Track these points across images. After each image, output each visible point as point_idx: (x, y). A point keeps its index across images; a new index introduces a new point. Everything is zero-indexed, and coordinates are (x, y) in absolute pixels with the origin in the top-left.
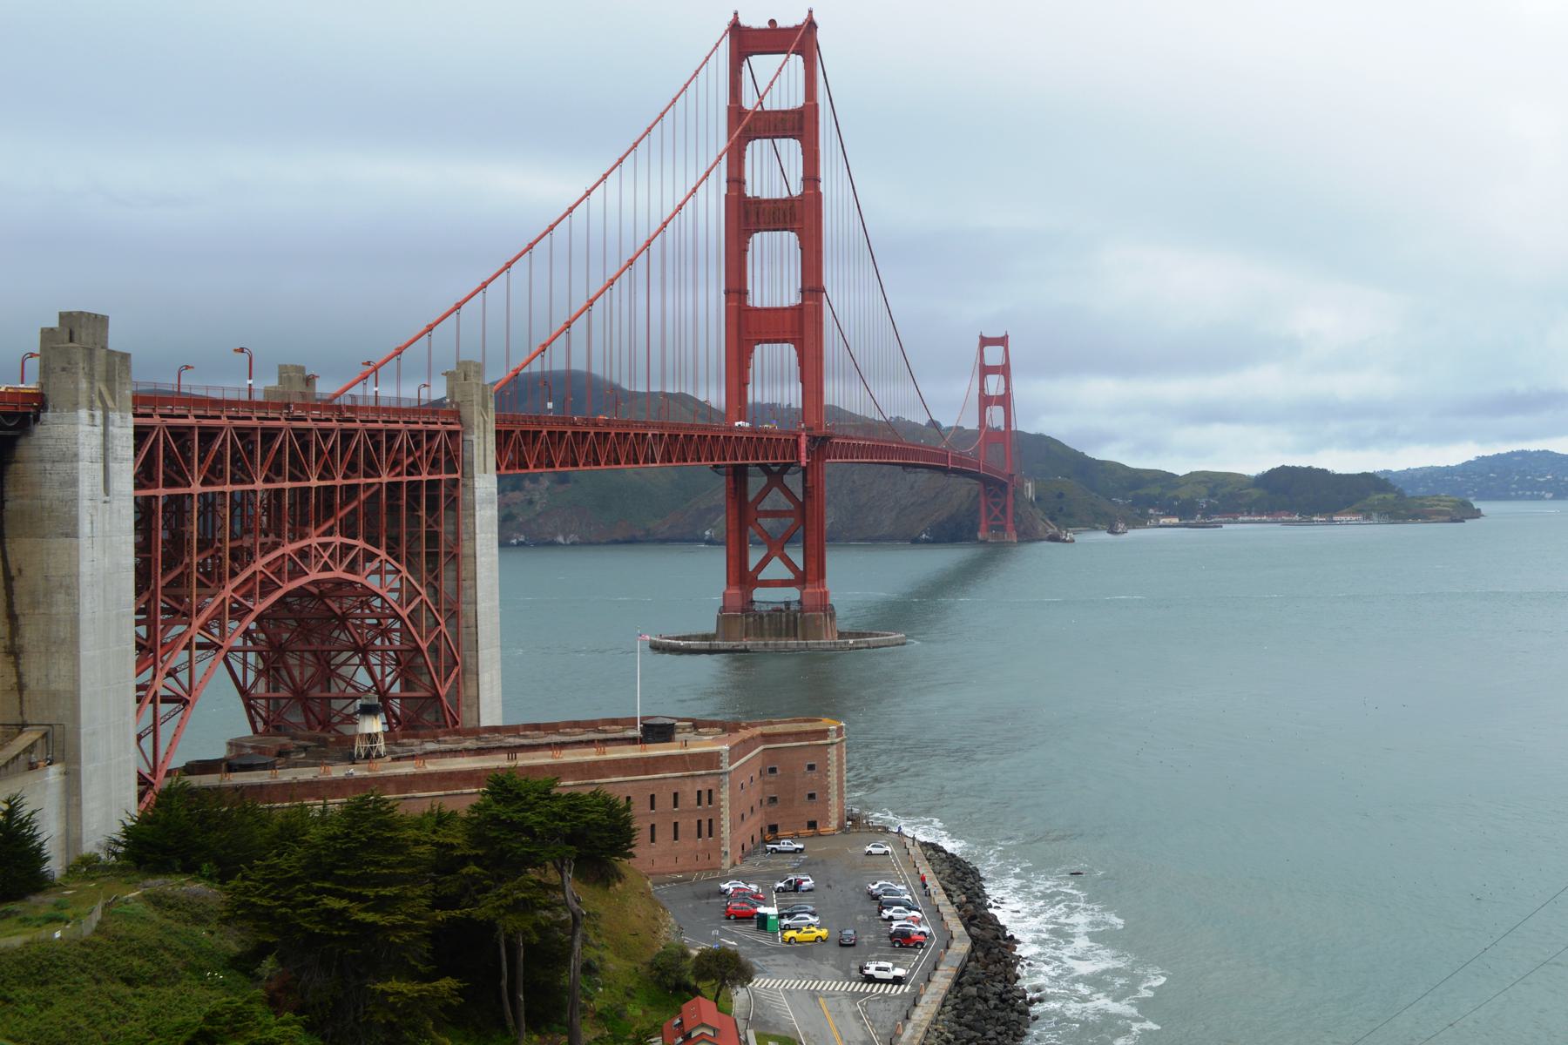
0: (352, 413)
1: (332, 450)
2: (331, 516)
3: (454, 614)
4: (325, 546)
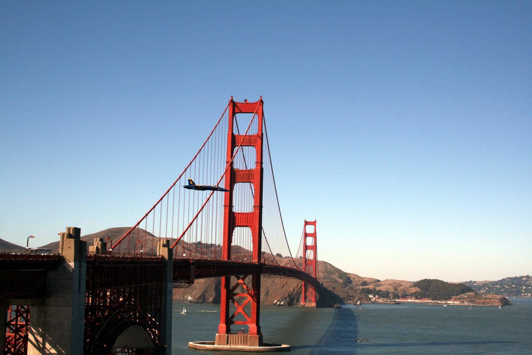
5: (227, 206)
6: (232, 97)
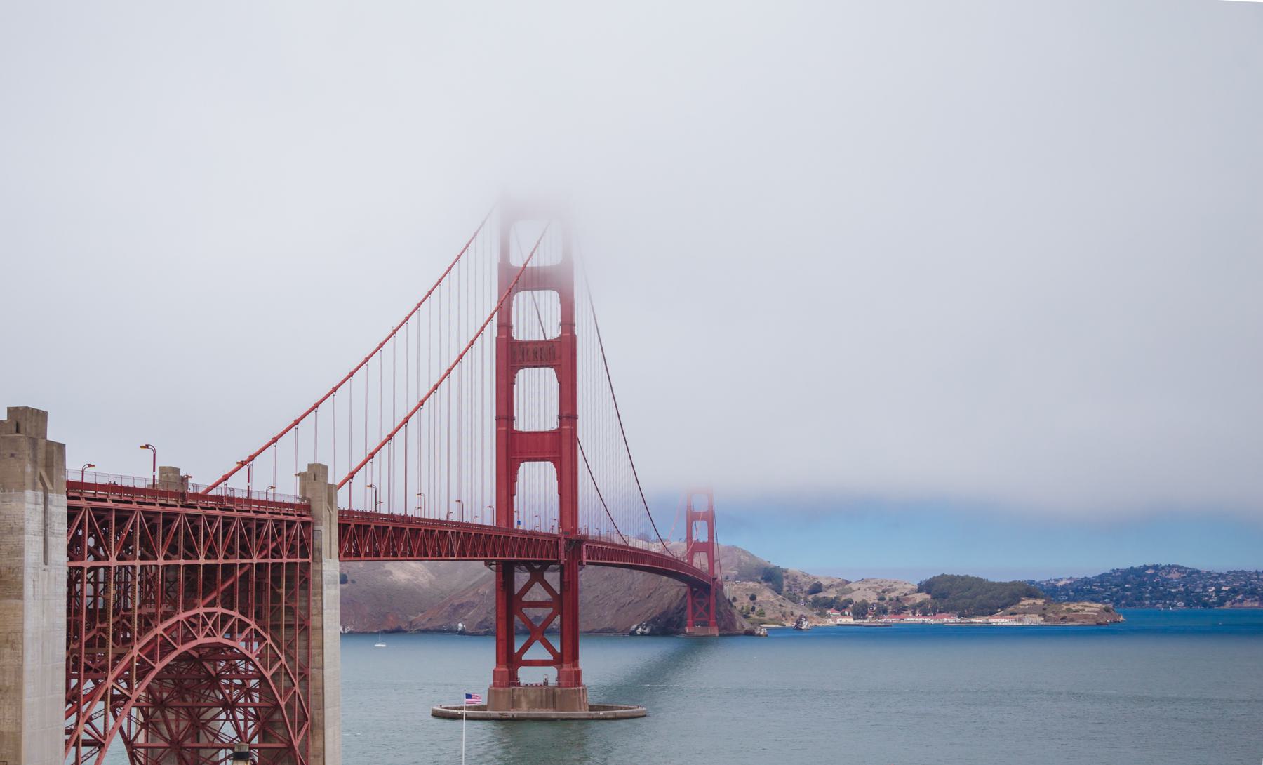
0: (231, 503)
2: (215, 590)
3: (304, 677)
4: (209, 615)
5: (503, 418)
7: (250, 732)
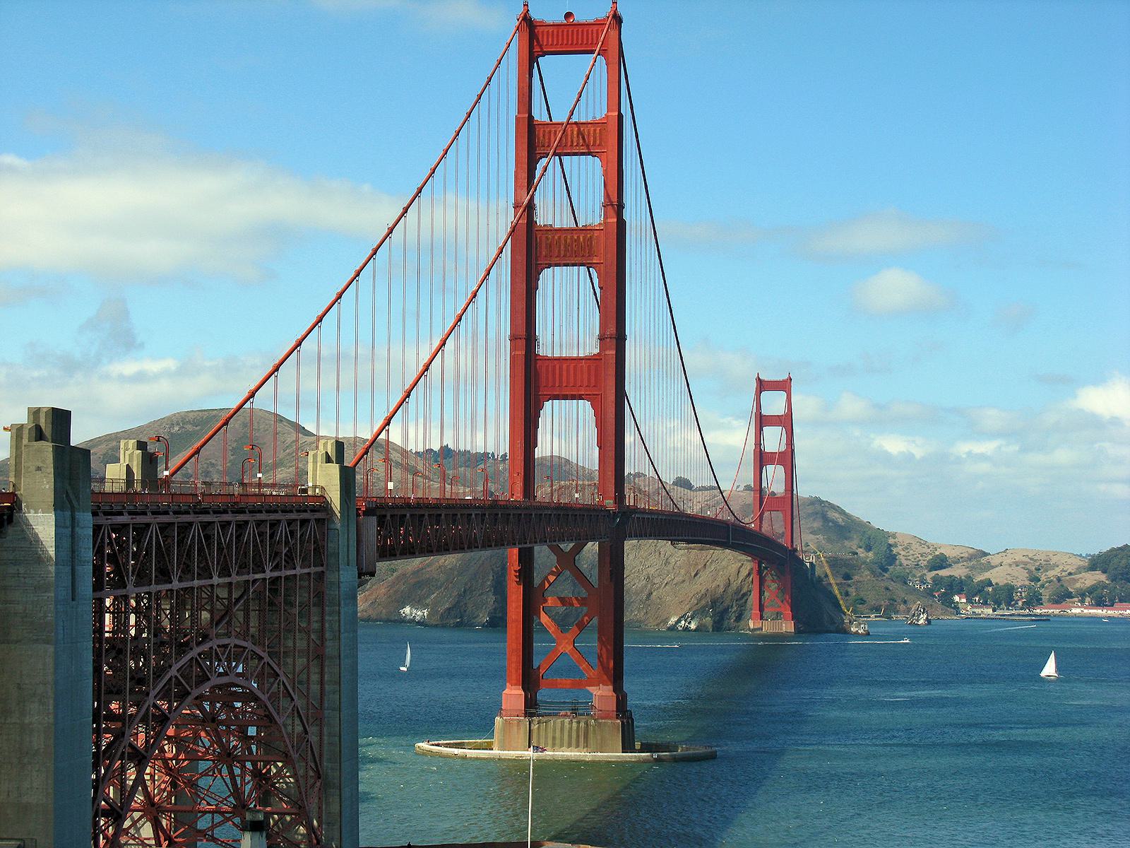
1: (229, 546)
6: (526, 5)
7: (248, 788)
